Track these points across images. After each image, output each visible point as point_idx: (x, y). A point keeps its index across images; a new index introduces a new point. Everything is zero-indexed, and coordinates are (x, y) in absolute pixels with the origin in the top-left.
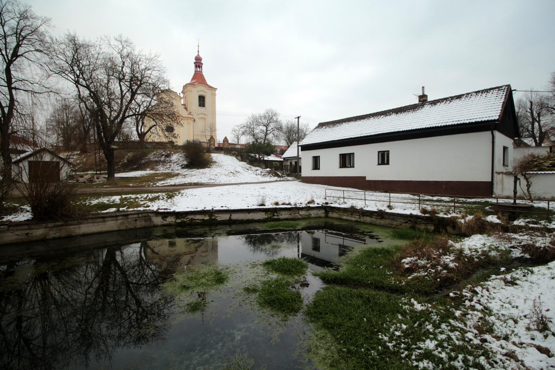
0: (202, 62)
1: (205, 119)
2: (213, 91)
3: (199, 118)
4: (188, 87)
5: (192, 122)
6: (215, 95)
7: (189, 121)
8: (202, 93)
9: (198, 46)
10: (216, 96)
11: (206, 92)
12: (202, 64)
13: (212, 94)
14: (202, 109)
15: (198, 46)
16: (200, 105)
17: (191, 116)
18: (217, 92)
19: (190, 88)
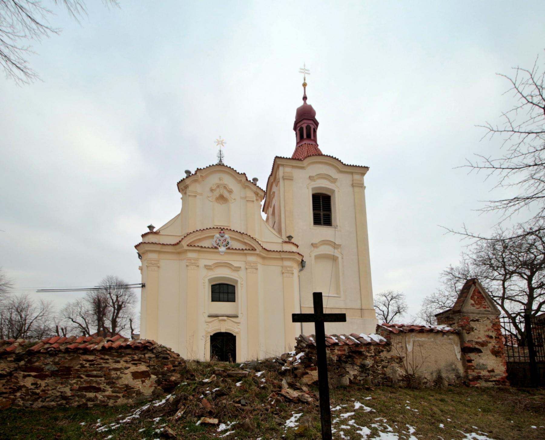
0: (317, 117)
1: (334, 259)
2: (357, 177)
3: (319, 257)
4: (281, 169)
5: (296, 268)
6: (362, 186)
7: (287, 263)
8: (323, 184)
9: (305, 85)
10: (366, 191)
11: (334, 181)
12: (317, 124)
13: (353, 186)
14: (323, 232)
15: (305, 85)
16: (317, 221)
17: (294, 249)
18: (367, 178)
19: (288, 170)
